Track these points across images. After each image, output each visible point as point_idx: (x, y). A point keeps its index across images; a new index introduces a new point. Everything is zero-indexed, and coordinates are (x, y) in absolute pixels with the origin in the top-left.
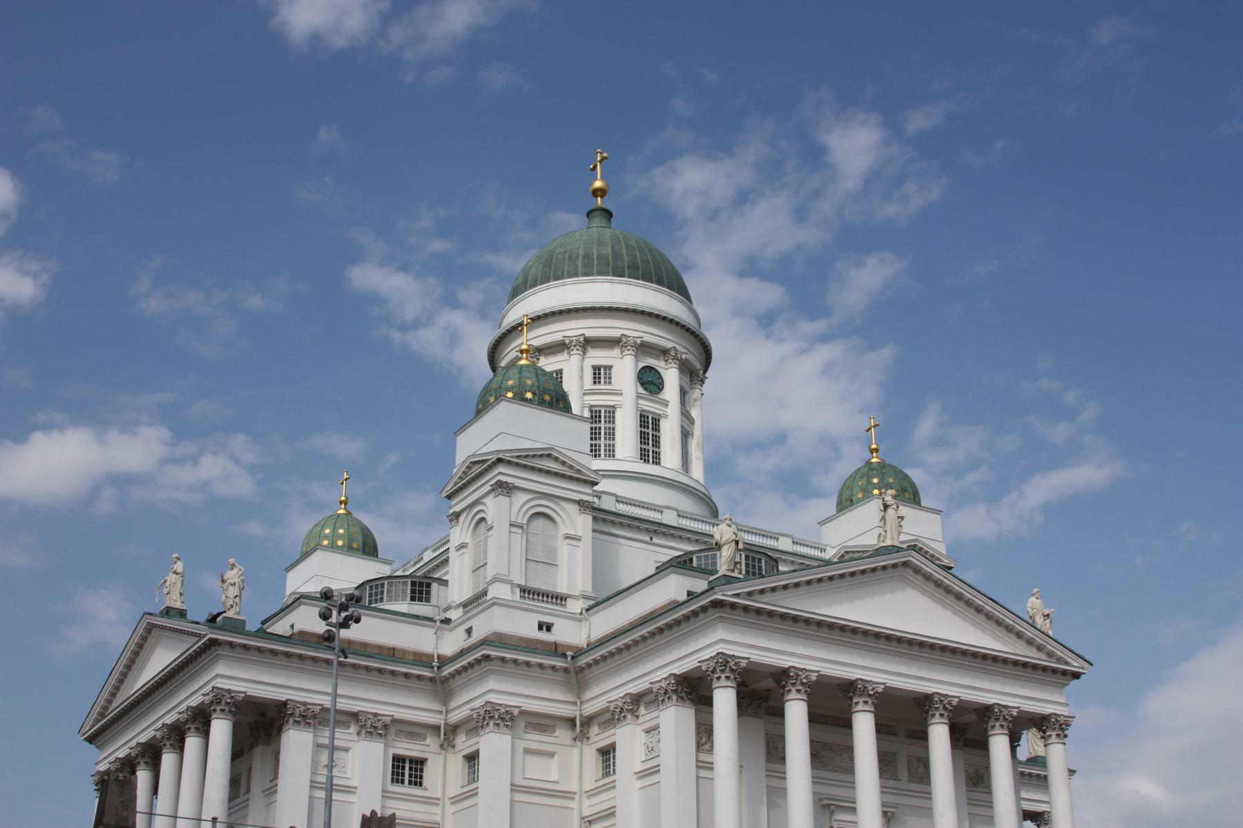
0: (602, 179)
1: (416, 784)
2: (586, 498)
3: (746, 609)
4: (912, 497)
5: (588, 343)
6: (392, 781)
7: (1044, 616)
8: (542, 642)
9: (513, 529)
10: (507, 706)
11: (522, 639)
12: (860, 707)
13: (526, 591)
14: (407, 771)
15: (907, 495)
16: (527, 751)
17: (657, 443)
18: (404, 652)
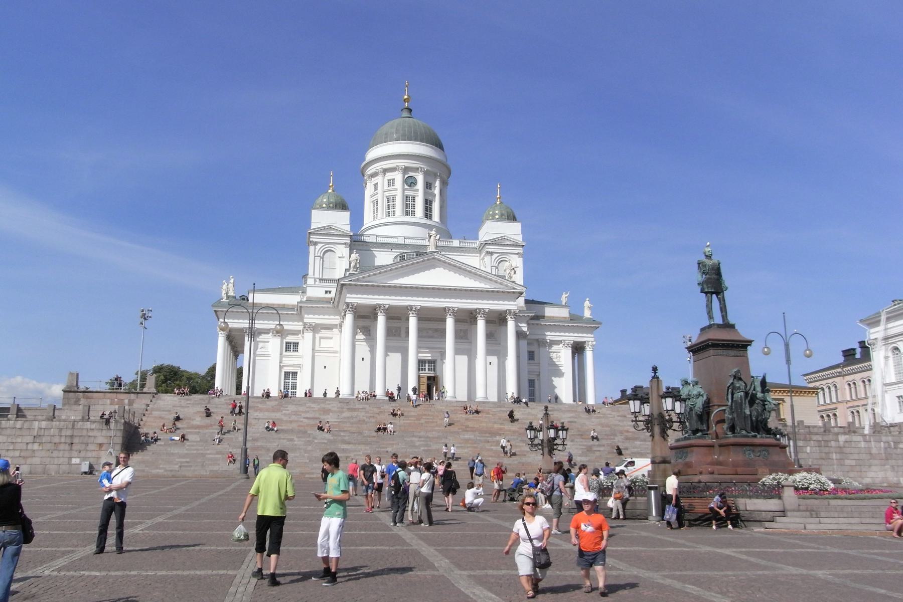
1: (295, 351)
3: (356, 285)
5: (385, 171)
6: (286, 351)
11: (317, 298)
13: (321, 280)
15: (503, 217)
16: (321, 338)
17: (414, 206)
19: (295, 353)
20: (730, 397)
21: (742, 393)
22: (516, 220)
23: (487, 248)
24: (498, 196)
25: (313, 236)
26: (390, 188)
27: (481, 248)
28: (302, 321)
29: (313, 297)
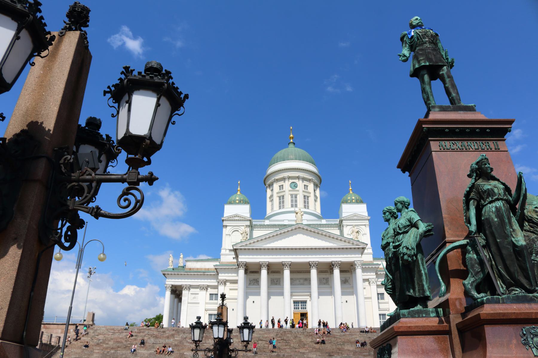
0: (292, 134)
2: (247, 224)
3: (245, 249)
4: (356, 201)
5: (277, 180)
6: (210, 299)
7: (356, 232)
8: (233, 262)
9: (227, 236)
10: (222, 279)
11: (228, 262)
12: (284, 269)
14: (214, 297)
15: (354, 201)
16: (230, 289)
17: (296, 201)
18: (211, 269)
19: (216, 301)
20: (473, 212)
21: (499, 204)
22: (362, 203)
23: (344, 223)
24: (351, 189)
25: (226, 221)
26: (280, 191)
27: (340, 224)
28: (218, 279)
29: (225, 262)
